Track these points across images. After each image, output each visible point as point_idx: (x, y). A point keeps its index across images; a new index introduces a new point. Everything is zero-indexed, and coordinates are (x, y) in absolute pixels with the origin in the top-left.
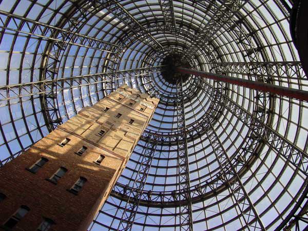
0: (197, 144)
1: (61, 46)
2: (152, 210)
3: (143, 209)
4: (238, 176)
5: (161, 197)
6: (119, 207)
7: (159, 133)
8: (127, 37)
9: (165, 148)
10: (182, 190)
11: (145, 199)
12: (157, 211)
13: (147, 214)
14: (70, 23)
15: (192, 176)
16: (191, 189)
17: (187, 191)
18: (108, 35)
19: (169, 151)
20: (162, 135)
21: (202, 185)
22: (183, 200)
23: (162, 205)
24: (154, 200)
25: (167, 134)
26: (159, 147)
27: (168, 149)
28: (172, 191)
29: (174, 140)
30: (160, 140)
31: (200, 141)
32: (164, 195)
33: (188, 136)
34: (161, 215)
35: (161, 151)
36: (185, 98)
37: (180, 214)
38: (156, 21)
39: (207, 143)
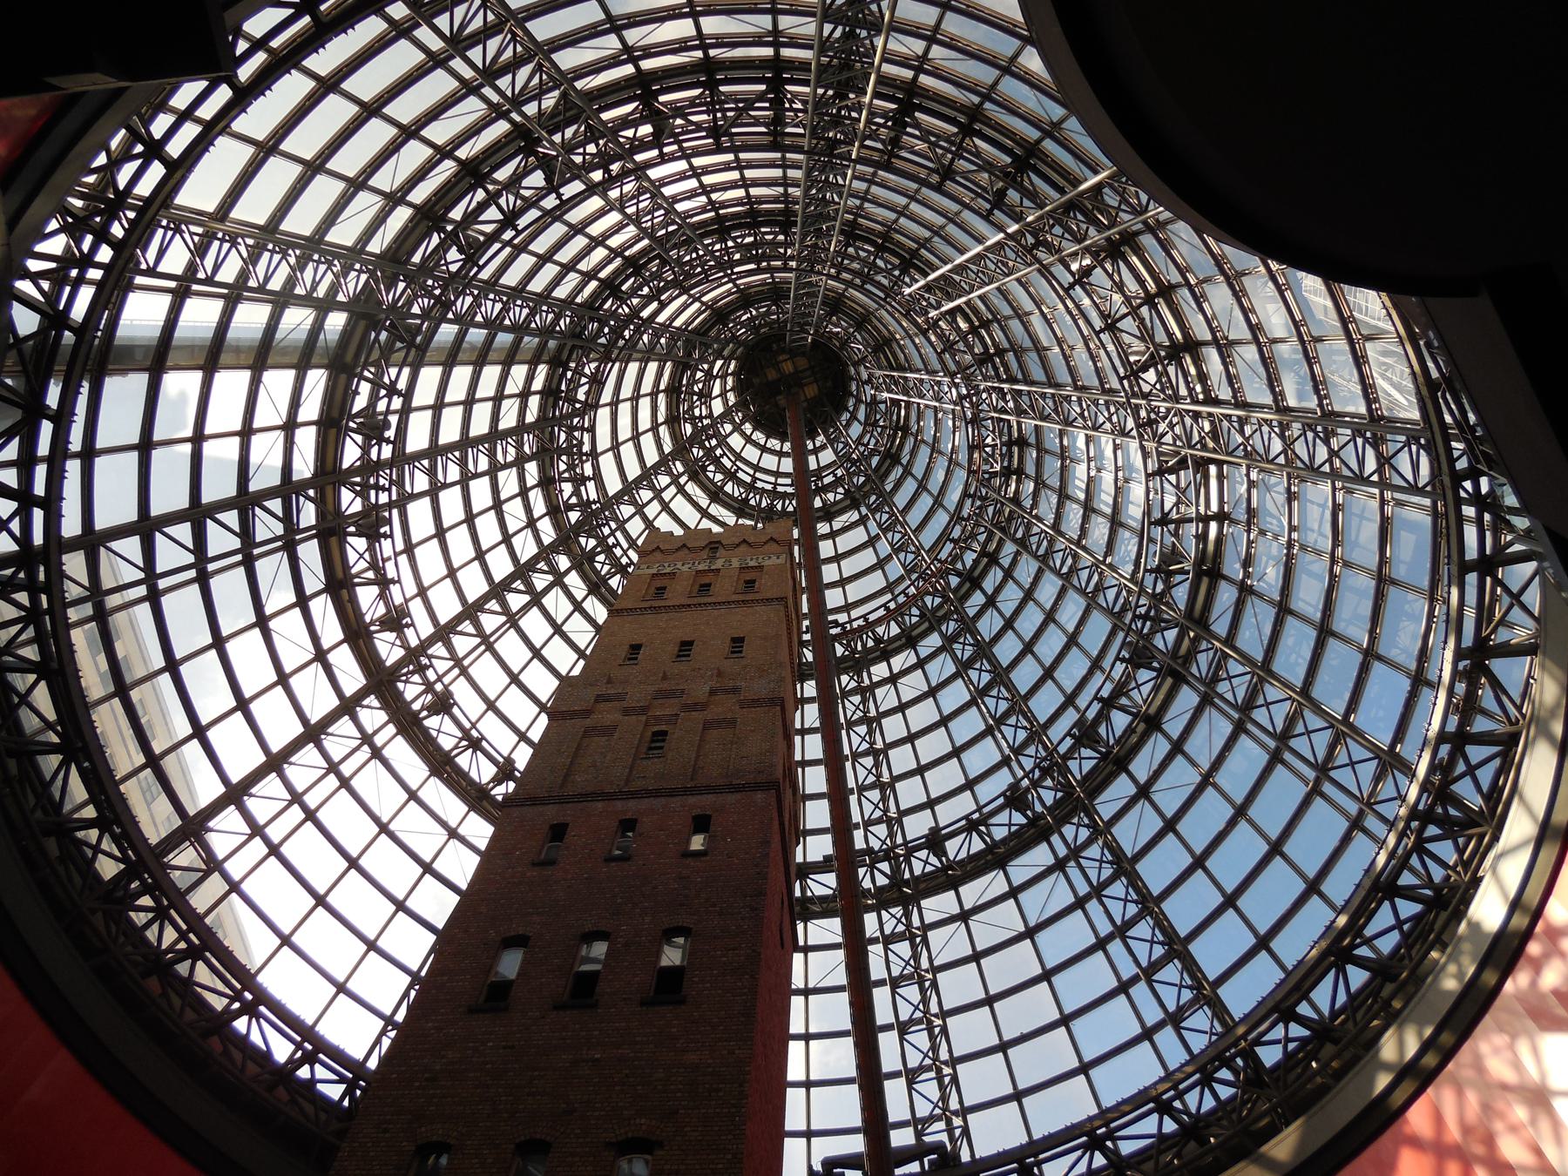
0: (998, 589)
1: (371, 525)
2: (972, 892)
4: (1197, 618)
5: (980, 834)
7: (855, 624)
8: (569, 374)
9: (898, 662)
10: (1032, 771)
11: (929, 868)
12: (992, 884)
13: (964, 916)
14: (359, 438)
15: (1045, 703)
16: (1062, 749)
17: (1053, 766)
18: (506, 404)
19: (921, 664)
20: (870, 626)
21: (1091, 715)
22: (1057, 803)
23: (996, 857)
24: (963, 855)
25: (882, 612)
26: (880, 671)
27: (913, 660)
28: (1003, 794)
29: (914, 620)
30: (870, 643)
31: (1000, 574)
32: (984, 820)
33: (954, 581)
34: (1013, 893)
35: (893, 679)
36: (875, 461)
37: (1075, 853)
38: (634, 265)
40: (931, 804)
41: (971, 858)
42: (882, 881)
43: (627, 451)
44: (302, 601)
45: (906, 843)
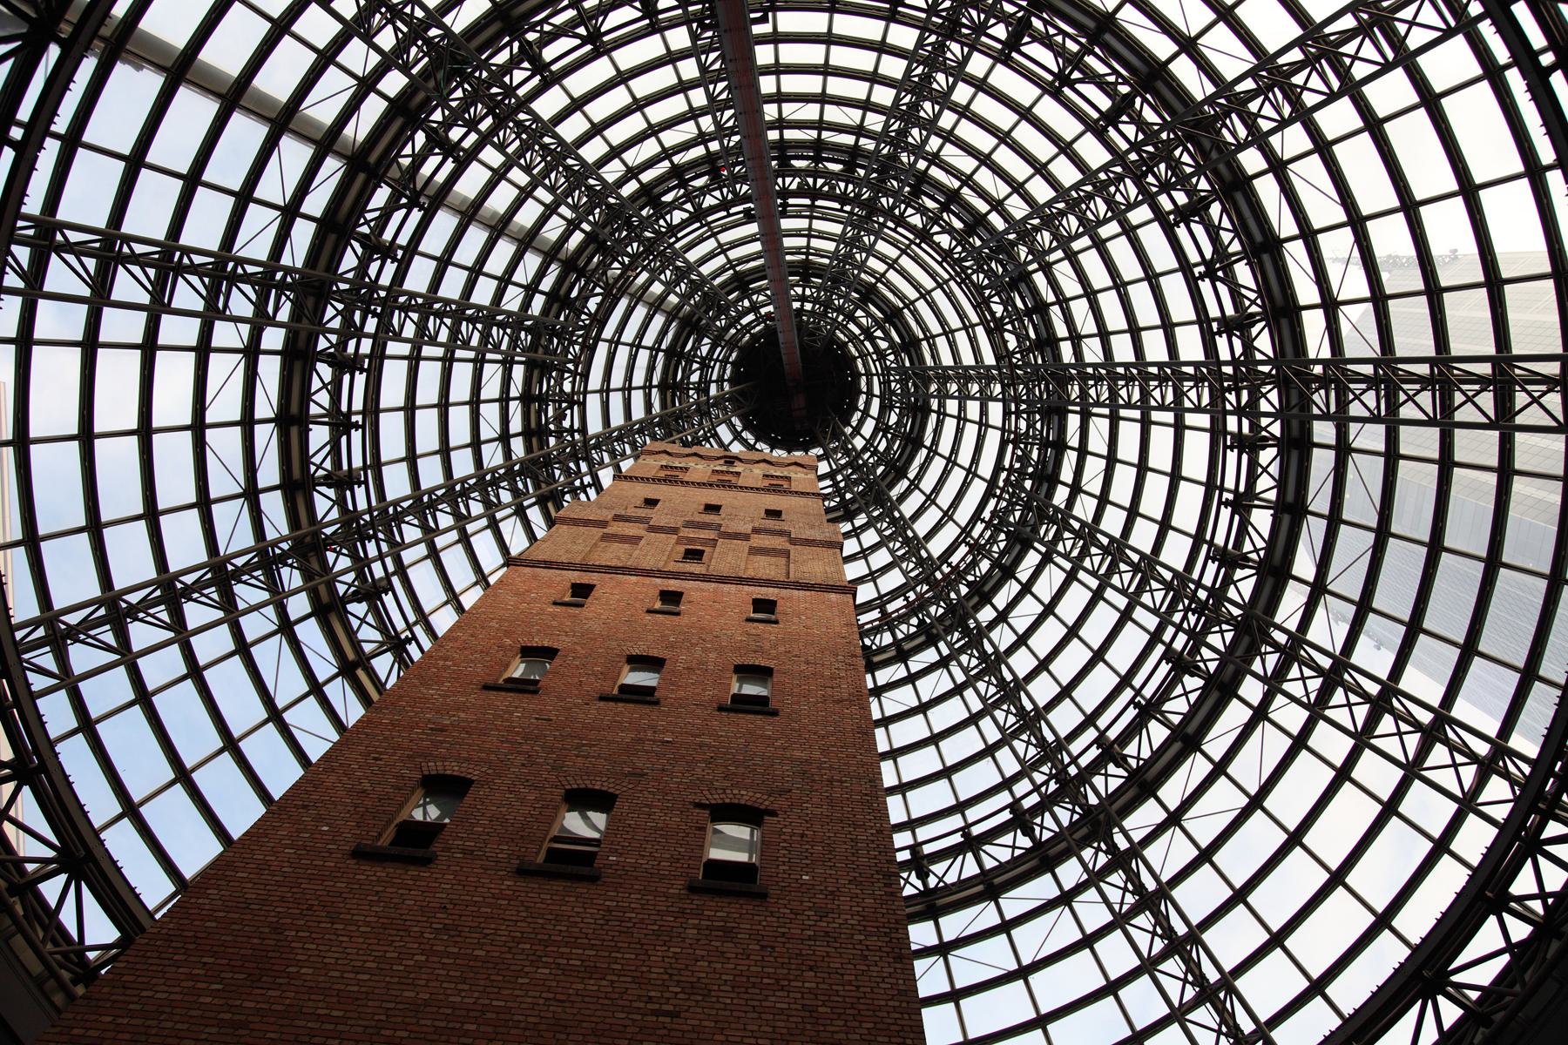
2: (1173, 791)
3: (1146, 816)
6: (1066, 898)
11: (1114, 784)
19: (1026, 589)
26: (986, 615)
30: (964, 590)
34: (1220, 768)
39: (1099, 429)
40: (1090, 720)
43: (616, 400)
44: (316, 689)
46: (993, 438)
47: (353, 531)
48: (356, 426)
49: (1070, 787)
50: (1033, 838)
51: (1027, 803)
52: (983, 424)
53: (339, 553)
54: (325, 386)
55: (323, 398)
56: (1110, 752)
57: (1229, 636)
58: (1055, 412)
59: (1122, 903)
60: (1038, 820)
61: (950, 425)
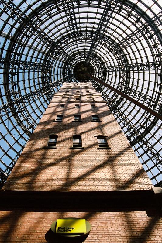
2: (152, 132)
3: (148, 136)
10: (153, 104)
11: (143, 131)
26: (119, 106)
30: (116, 103)
40: (138, 122)
41: (150, 125)
42: (136, 137)
45: (136, 128)
46: (118, 78)
47: (17, 102)
48: (16, 84)
49: (135, 133)
50: (131, 141)
51: (129, 136)
52: (116, 76)
53: (16, 105)
54: (11, 78)
55: (10, 80)
56: (142, 127)
57: (160, 106)
58: (128, 72)
59: (146, 150)
60: (131, 138)
61: (110, 76)
